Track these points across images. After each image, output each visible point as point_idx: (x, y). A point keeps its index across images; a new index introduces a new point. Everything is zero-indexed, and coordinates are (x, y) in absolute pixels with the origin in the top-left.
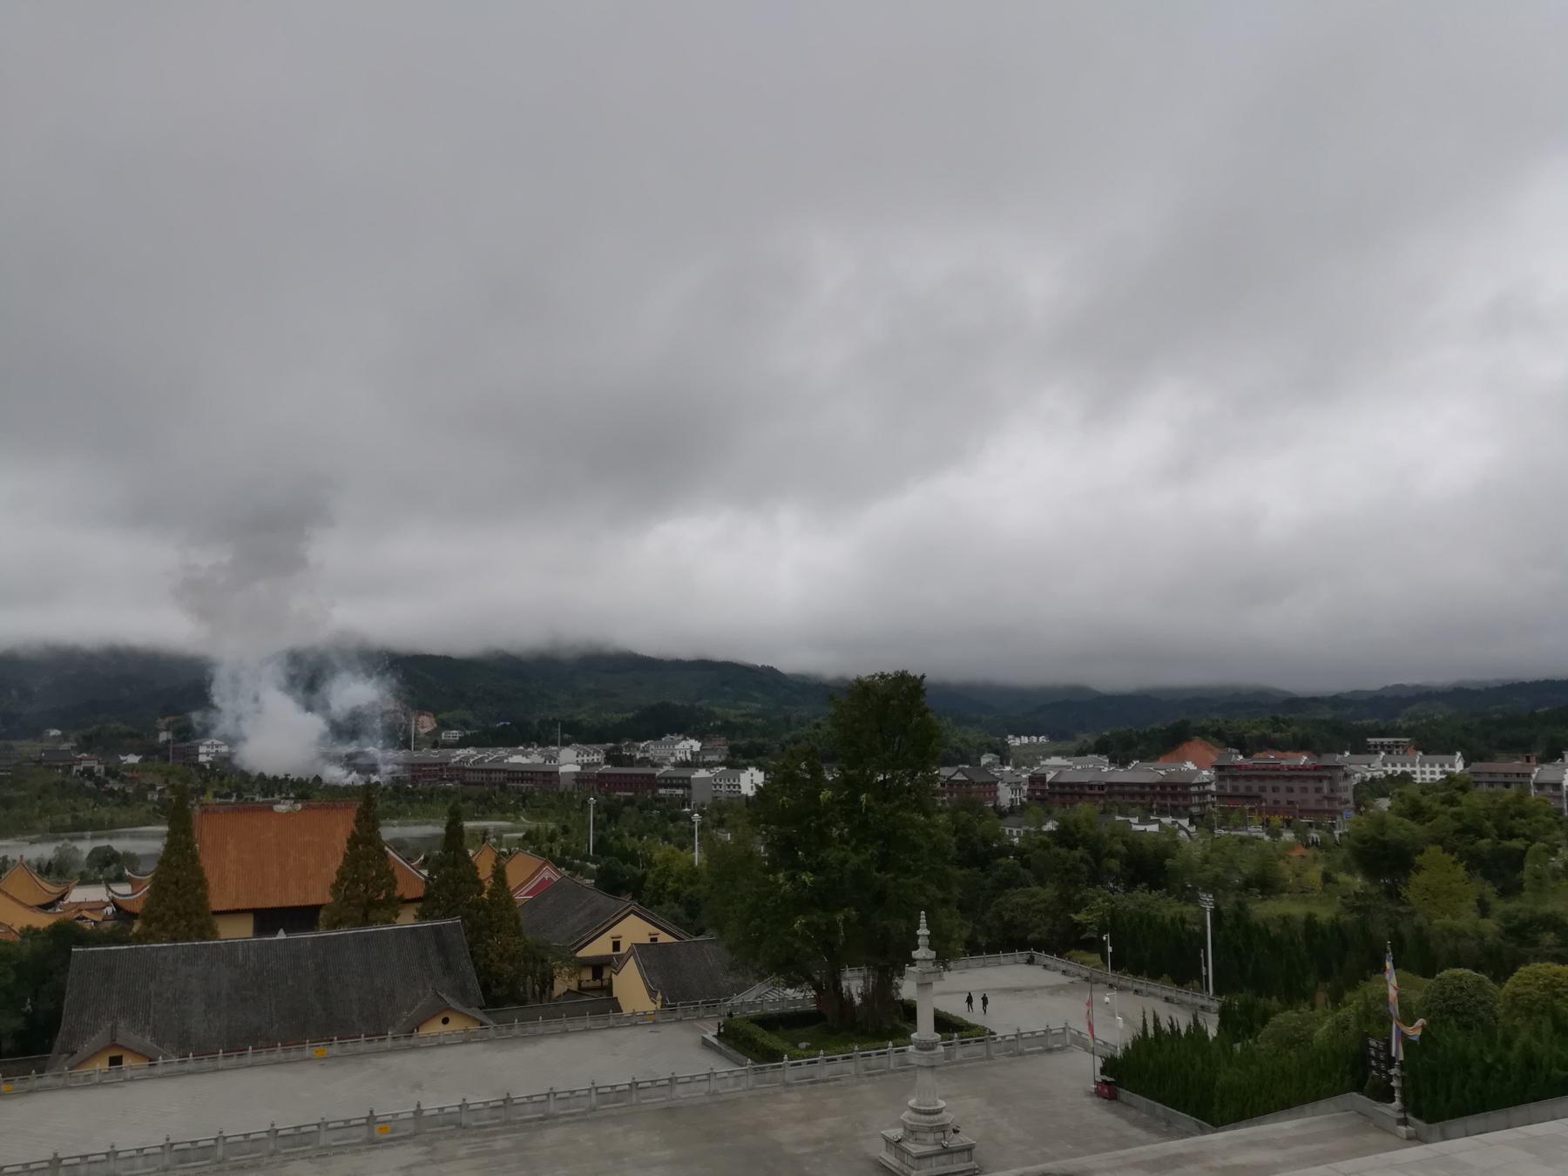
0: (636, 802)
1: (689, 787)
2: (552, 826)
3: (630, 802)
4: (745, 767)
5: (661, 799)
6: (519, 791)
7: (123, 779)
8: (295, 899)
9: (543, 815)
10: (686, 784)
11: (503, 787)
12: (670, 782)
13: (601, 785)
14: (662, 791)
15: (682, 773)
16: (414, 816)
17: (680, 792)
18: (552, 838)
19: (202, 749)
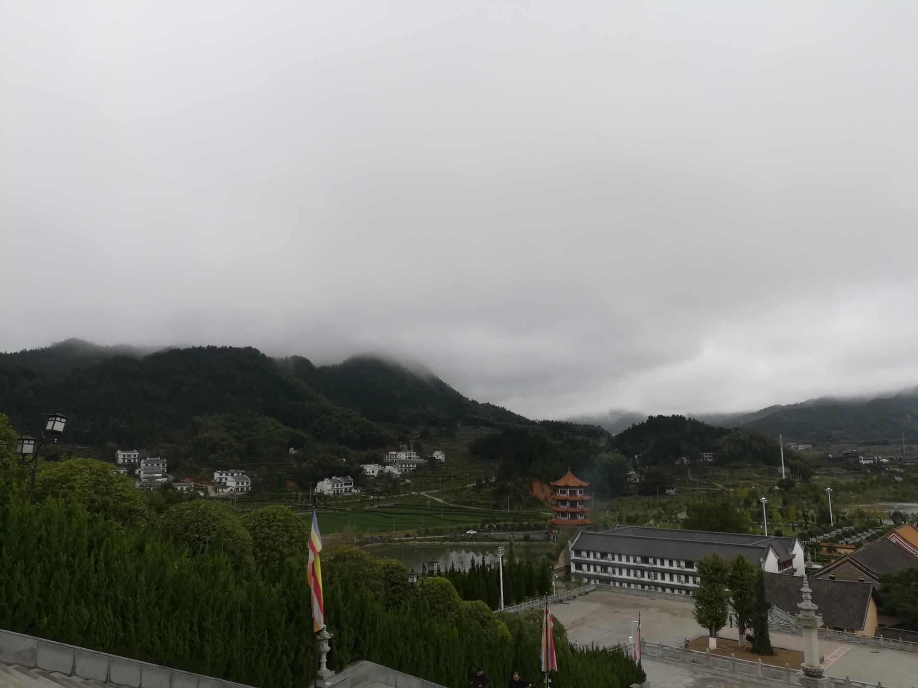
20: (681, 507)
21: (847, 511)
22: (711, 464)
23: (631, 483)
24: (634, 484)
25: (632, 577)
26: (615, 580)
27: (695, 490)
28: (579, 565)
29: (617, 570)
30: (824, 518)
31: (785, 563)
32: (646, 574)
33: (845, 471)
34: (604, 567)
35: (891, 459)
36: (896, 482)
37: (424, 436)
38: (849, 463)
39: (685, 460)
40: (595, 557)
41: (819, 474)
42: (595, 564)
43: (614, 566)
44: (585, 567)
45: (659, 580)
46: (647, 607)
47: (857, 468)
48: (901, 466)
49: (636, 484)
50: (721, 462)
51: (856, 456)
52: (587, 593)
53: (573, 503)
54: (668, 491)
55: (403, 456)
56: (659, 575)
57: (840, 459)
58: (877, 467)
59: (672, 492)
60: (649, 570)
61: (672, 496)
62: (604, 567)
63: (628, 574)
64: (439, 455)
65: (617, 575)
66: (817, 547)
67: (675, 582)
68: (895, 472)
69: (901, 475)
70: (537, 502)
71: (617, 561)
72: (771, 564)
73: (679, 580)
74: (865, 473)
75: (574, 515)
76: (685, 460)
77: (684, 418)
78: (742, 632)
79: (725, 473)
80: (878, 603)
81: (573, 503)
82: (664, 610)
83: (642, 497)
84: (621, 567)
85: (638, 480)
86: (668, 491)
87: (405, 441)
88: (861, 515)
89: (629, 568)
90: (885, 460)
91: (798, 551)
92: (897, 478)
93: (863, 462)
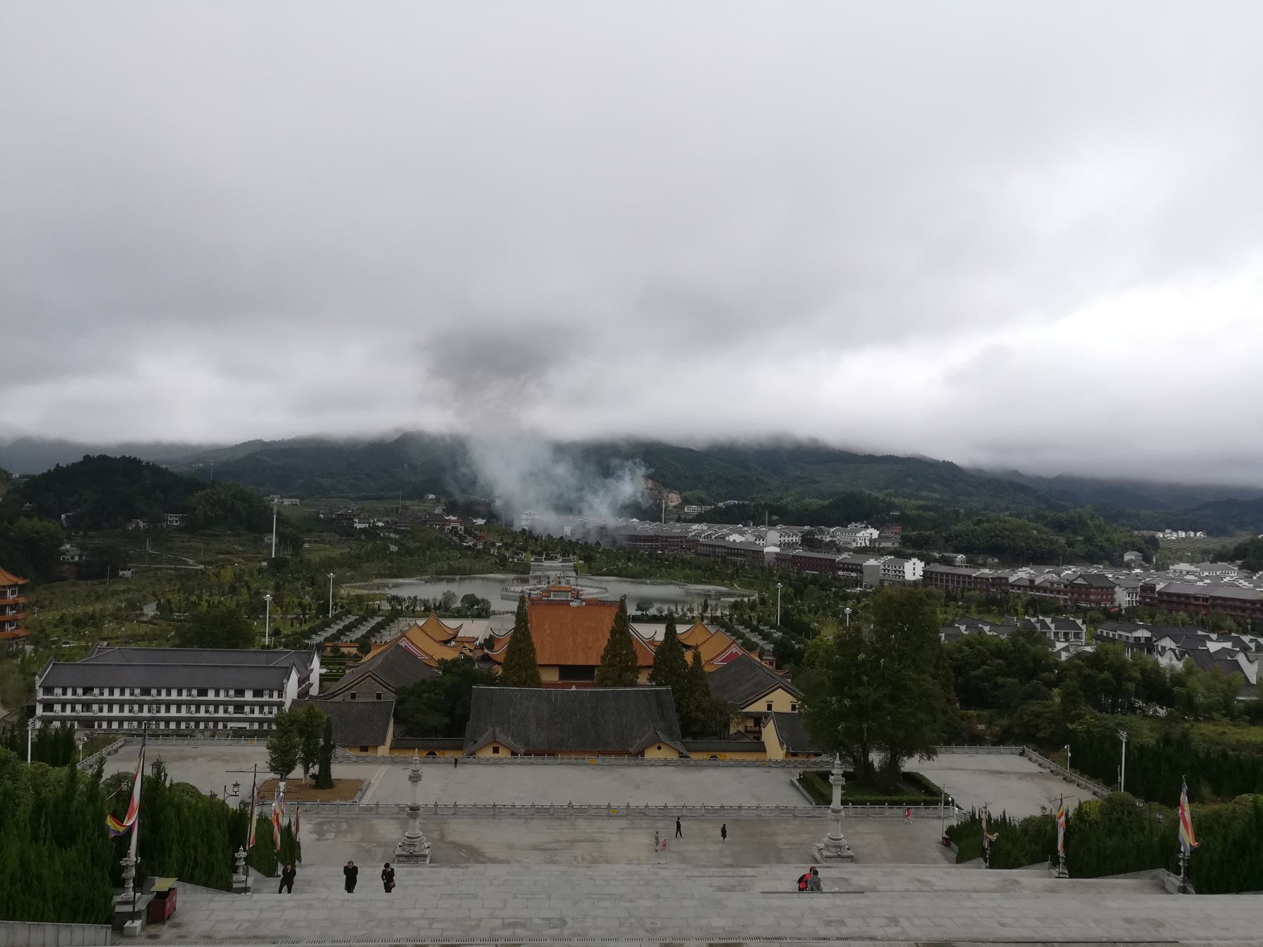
0: (814, 579)
1: (862, 572)
2: (755, 597)
3: (814, 581)
4: (908, 557)
5: (838, 579)
6: (735, 564)
7: (475, 537)
9: (749, 585)
11: (724, 561)
12: (846, 567)
13: (794, 564)
14: (840, 573)
15: (856, 559)
16: (661, 577)
17: (854, 575)
18: (752, 606)
19: (524, 517)
20: (145, 597)
22: (179, 529)
23: (65, 562)
24: (69, 563)
25: (126, 713)
26: (101, 719)
27: (158, 569)
28: (48, 706)
29: (105, 707)
32: (146, 708)
33: (337, 537)
34: (87, 706)
35: (386, 522)
36: (392, 553)
38: (341, 527)
39: (141, 524)
40: (74, 693)
41: (309, 542)
42: (73, 703)
43: (101, 703)
44: (58, 707)
45: (163, 713)
46: (194, 758)
47: (349, 533)
48: (396, 532)
49: (76, 564)
50: (191, 528)
51: (350, 518)
52: (116, 751)
54: (121, 573)
56: (163, 708)
57: (332, 520)
58: (371, 533)
59: (128, 573)
60: (150, 703)
61: (127, 579)
62: (87, 706)
63: (121, 710)
65: (105, 713)
67: (184, 713)
68: (390, 539)
69: (395, 542)
71: (106, 696)
73: (189, 711)
74: (359, 539)
76: (141, 524)
77: (140, 462)
78: (306, 772)
82: (213, 758)
83: (82, 583)
84: (110, 704)
85: (77, 558)
86: (121, 573)
89: (122, 704)
90: (380, 524)
92: (394, 548)
93: (358, 526)
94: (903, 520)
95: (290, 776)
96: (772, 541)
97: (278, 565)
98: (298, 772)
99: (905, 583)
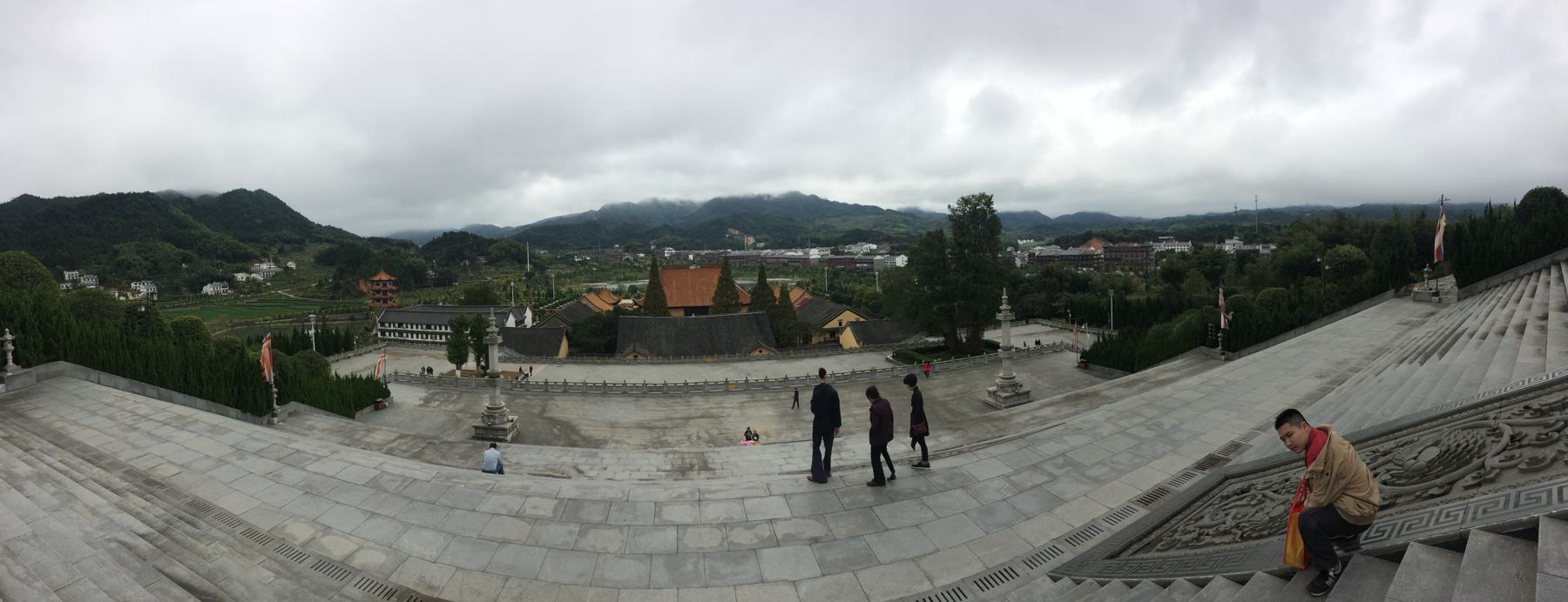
8: (699, 304)
10: (871, 262)
21: (564, 290)
30: (550, 294)
31: (520, 322)
37: (281, 251)
50: (490, 263)
53: (385, 293)
55: (264, 266)
64: (292, 265)
66: (543, 312)
70: (362, 294)
72: (511, 322)
75: (385, 301)
79: (492, 270)
80: (569, 339)
81: (385, 293)
87: (266, 256)
88: (571, 291)
91: (529, 314)
94: (888, 239)
95: (464, 367)
96: (815, 253)
97: (529, 275)
98: (471, 364)
99: (899, 268)
